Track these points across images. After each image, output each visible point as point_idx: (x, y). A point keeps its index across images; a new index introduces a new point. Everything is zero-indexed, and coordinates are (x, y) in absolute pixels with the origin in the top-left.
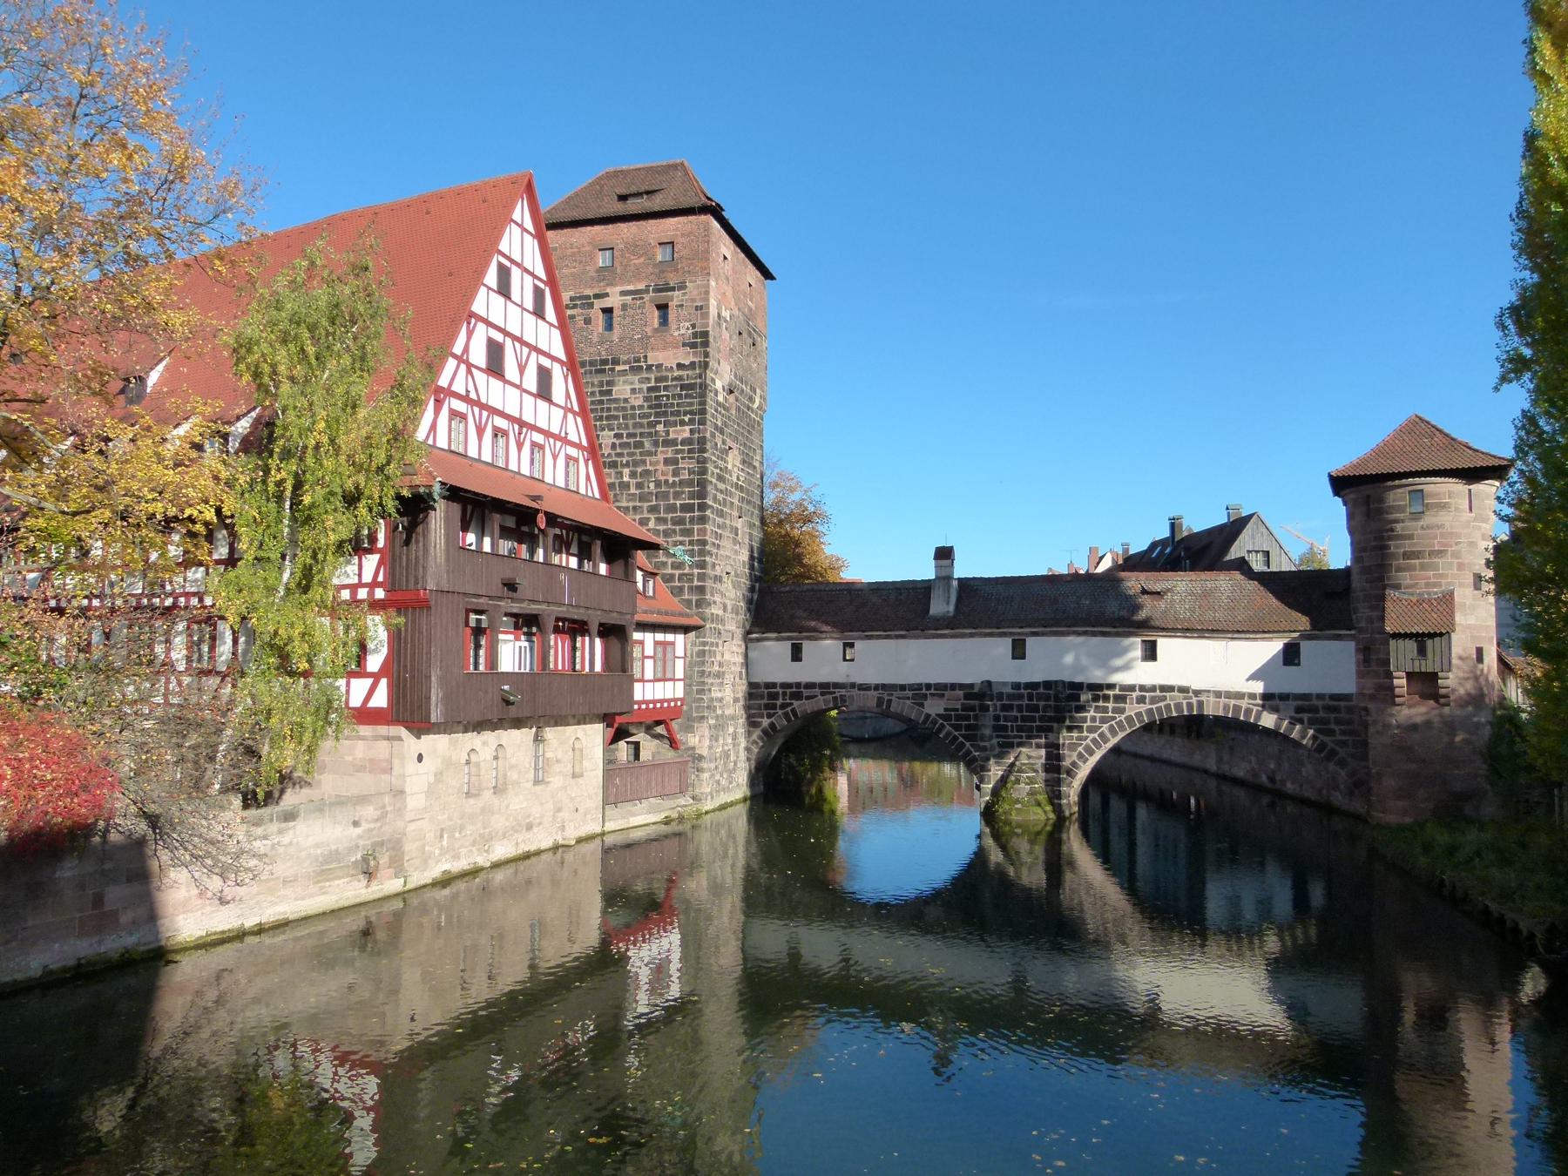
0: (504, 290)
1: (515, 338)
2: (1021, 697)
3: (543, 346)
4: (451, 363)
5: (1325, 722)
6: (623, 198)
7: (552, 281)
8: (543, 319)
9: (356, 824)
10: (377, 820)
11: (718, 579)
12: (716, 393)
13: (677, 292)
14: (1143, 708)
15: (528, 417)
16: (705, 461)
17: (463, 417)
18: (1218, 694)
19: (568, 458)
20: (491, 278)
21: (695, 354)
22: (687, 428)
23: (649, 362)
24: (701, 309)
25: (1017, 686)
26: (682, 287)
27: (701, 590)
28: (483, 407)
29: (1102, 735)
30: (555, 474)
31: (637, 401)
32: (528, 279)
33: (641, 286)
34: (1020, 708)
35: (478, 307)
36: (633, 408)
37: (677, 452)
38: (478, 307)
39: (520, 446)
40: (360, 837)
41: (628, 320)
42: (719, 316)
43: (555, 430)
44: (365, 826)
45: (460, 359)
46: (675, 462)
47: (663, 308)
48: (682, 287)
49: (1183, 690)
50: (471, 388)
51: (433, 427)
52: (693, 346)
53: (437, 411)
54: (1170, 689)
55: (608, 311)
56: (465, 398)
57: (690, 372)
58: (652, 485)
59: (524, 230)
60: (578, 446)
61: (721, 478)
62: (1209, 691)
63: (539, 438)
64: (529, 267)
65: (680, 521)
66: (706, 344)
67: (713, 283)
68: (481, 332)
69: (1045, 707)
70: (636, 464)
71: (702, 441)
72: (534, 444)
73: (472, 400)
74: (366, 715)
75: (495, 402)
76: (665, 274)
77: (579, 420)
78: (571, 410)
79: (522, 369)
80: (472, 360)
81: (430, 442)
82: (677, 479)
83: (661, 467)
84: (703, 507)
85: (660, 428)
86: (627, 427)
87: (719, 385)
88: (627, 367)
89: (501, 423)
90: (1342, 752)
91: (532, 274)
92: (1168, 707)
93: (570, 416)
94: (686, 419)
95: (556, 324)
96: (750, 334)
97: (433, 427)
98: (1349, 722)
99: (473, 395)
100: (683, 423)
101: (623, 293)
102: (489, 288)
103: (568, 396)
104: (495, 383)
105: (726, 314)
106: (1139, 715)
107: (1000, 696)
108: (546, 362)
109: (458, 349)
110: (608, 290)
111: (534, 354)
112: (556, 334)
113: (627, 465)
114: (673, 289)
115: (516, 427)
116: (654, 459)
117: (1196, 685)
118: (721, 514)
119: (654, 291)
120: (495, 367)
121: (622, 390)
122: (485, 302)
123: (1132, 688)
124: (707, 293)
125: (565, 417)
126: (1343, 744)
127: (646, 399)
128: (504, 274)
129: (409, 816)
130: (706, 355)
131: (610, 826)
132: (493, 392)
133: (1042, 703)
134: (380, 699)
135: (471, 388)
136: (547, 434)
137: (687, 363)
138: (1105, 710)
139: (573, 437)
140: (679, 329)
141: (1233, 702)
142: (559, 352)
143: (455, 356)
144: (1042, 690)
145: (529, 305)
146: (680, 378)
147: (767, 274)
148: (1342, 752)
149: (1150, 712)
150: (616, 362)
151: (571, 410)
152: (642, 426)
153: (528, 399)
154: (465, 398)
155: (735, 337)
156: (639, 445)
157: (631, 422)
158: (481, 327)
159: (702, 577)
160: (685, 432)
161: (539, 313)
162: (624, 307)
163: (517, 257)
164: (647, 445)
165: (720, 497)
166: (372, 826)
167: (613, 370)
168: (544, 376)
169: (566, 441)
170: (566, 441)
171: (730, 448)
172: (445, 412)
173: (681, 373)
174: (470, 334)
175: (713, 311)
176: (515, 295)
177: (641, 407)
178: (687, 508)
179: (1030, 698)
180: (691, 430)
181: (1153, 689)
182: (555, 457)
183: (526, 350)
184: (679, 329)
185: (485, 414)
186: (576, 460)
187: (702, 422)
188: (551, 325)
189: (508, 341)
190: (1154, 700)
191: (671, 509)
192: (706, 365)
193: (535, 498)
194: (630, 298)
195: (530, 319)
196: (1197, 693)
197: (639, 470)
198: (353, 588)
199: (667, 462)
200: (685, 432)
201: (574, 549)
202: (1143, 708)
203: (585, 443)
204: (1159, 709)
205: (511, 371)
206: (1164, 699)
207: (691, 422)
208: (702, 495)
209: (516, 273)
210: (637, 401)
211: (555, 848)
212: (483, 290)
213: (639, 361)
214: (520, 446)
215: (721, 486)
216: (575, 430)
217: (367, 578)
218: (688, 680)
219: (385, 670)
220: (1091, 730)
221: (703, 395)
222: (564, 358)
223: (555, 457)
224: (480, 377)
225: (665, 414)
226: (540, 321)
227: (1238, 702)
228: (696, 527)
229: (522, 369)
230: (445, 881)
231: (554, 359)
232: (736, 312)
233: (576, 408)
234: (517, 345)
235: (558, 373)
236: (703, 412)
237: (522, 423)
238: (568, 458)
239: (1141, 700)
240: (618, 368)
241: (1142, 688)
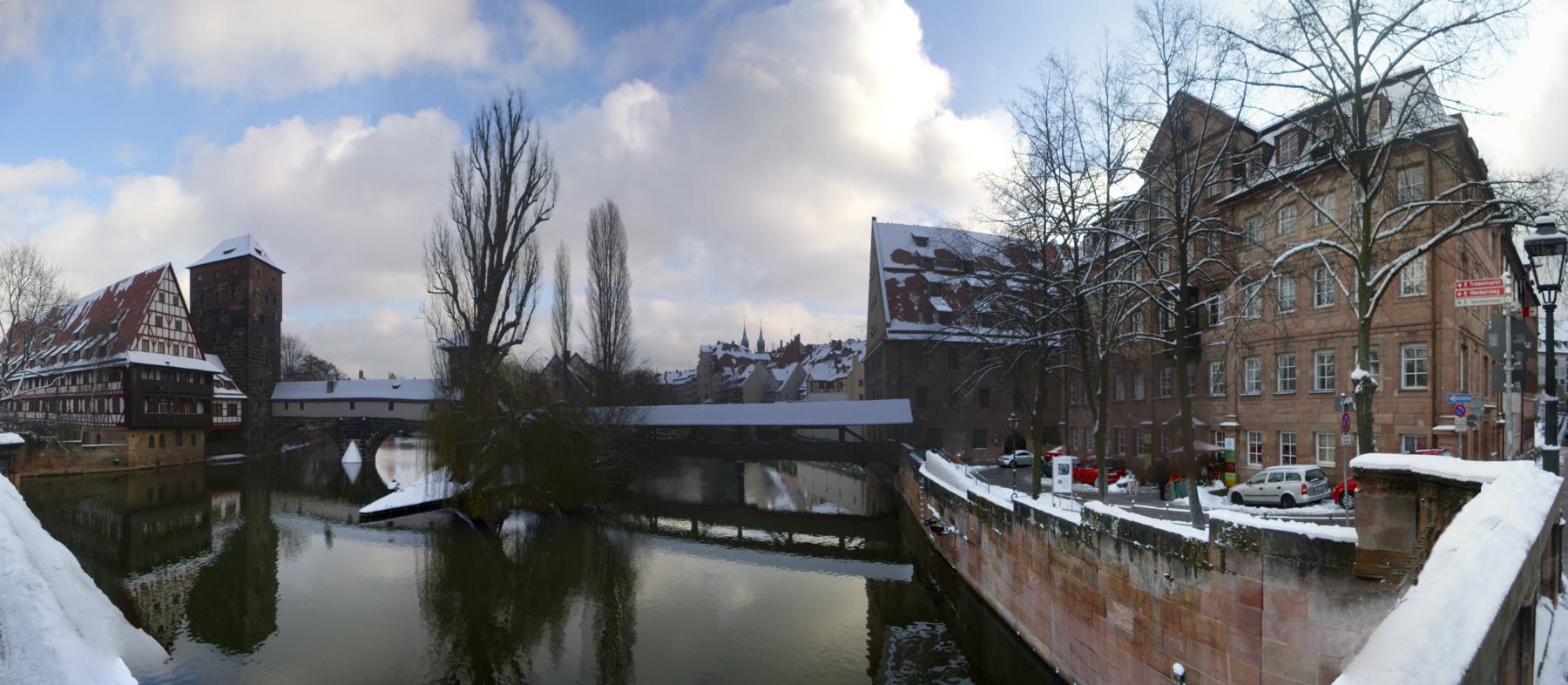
0: (162, 300)
1: (166, 314)
3: (178, 314)
4: (143, 326)
6: (226, 253)
12: (254, 318)
15: (172, 337)
17: (148, 341)
19: (189, 348)
20: (157, 298)
24: (247, 290)
28: (154, 337)
31: (227, 323)
33: (226, 284)
35: (152, 308)
39: (169, 346)
42: (255, 291)
43: (183, 339)
45: (146, 325)
47: (233, 291)
53: (138, 340)
55: (217, 293)
59: (169, 280)
60: (193, 343)
61: (255, 347)
64: (171, 291)
67: (251, 281)
68: (153, 316)
72: (174, 345)
74: (119, 424)
75: (159, 334)
79: (169, 323)
85: (234, 332)
87: (255, 315)
99: (151, 334)
103: (188, 328)
104: (159, 330)
105: (258, 290)
108: (179, 319)
109: (145, 321)
112: (183, 310)
121: (222, 320)
122: (156, 306)
125: (187, 336)
131: (207, 460)
132: (159, 332)
134: (123, 421)
136: (180, 341)
139: (190, 340)
142: (184, 315)
145: (172, 303)
153: (172, 333)
154: (148, 335)
155: (263, 299)
158: (154, 313)
160: (241, 333)
161: (176, 304)
163: (166, 289)
169: (187, 342)
170: (187, 342)
172: (141, 341)
174: (149, 316)
175: (251, 288)
176: (166, 301)
178: (243, 359)
182: (183, 348)
186: (192, 348)
192: (248, 309)
193: (167, 363)
195: (172, 308)
198: (117, 391)
199: (237, 344)
200: (241, 333)
201: (192, 375)
203: (195, 342)
205: (165, 324)
209: (166, 294)
210: (227, 323)
211: (184, 465)
212: (153, 303)
214: (169, 346)
216: (191, 338)
217: (119, 388)
218: (242, 416)
219: (124, 413)
222: (186, 316)
223: (183, 348)
224: (153, 329)
229: (169, 323)
230: (142, 469)
231: (182, 318)
237: (169, 339)
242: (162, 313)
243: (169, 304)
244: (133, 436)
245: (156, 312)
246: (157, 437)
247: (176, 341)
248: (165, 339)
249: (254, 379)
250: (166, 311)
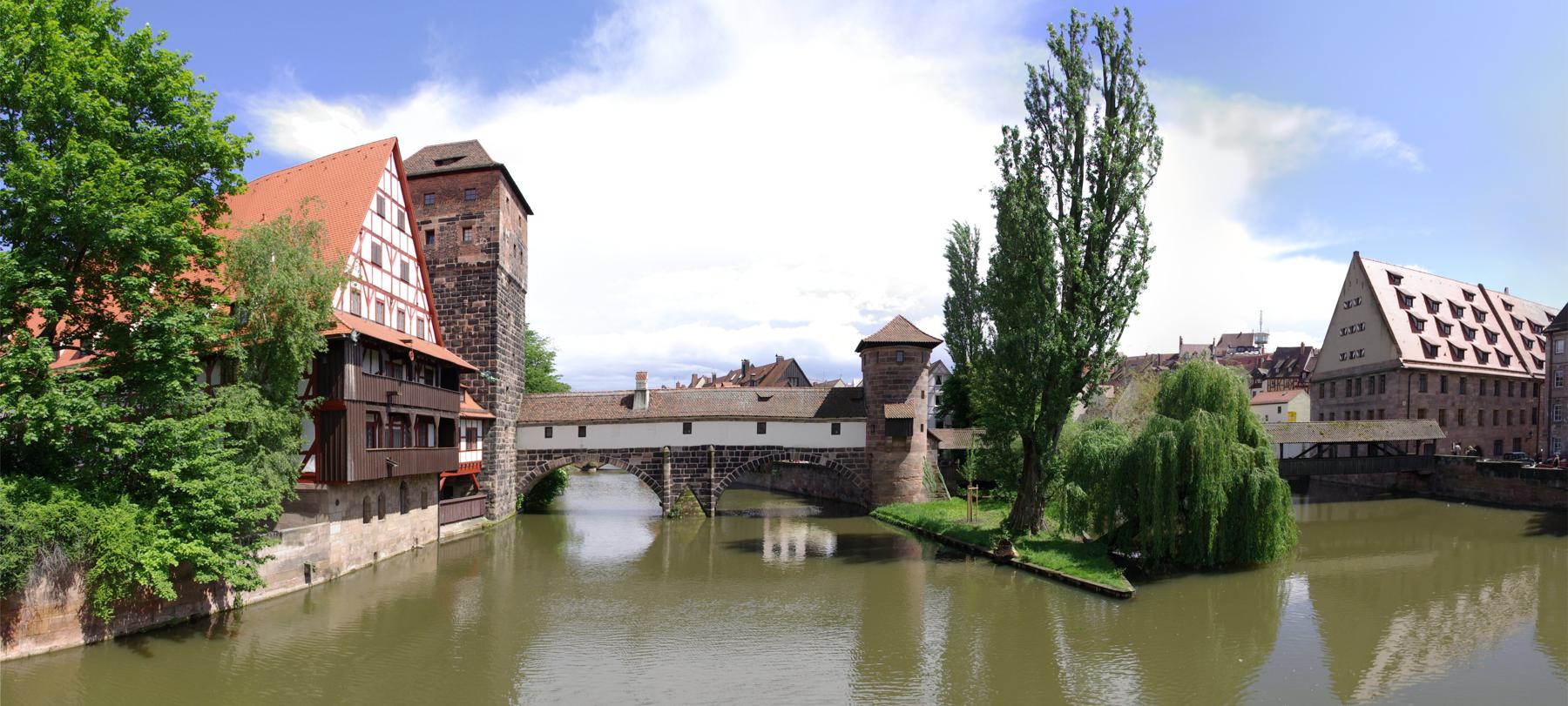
2: (688, 454)
3: (404, 248)
5: (851, 461)
6: (439, 163)
7: (407, 209)
8: (404, 232)
9: (301, 544)
10: (313, 541)
11: (502, 391)
13: (477, 220)
14: (757, 458)
15: (396, 293)
16: (493, 322)
18: (798, 450)
20: (374, 206)
21: (490, 257)
22: (484, 302)
23: (459, 262)
24: (495, 229)
25: (685, 448)
26: (481, 216)
27: (493, 398)
29: (734, 473)
30: (411, 329)
32: (395, 207)
33: (454, 215)
34: (687, 461)
35: (366, 224)
36: (448, 290)
37: (478, 316)
38: (366, 224)
40: (304, 551)
41: (445, 237)
42: (504, 233)
44: (306, 545)
46: (476, 322)
48: (481, 216)
49: (780, 448)
50: (363, 274)
51: (341, 299)
52: (488, 252)
53: (344, 288)
54: (773, 447)
56: (359, 280)
57: (486, 268)
58: (460, 337)
60: (423, 311)
62: (793, 448)
63: (402, 306)
64: (395, 199)
65: (479, 357)
66: (497, 251)
67: (501, 214)
68: (368, 238)
69: (702, 459)
70: (449, 324)
71: (494, 311)
73: (363, 282)
75: (377, 283)
76: (470, 208)
77: (424, 295)
78: (420, 289)
80: (363, 257)
81: (340, 308)
82: (477, 333)
83: (467, 326)
84: (494, 349)
86: (443, 302)
88: (444, 265)
89: (381, 296)
90: (858, 476)
91: (396, 203)
92: (771, 457)
93: (419, 292)
94: (484, 296)
95: (411, 235)
96: (519, 246)
97: (341, 299)
98: (862, 461)
99: (364, 279)
100: (481, 299)
101: (440, 220)
102: (373, 211)
103: (418, 280)
105: (508, 233)
106: (755, 462)
107: (676, 454)
108: (405, 259)
109: (355, 250)
110: (431, 218)
111: (398, 254)
112: (411, 241)
113: (444, 324)
114: (475, 217)
115: (389, 299)
116: (462, 320)
117: (785, 446)
118: (504, 353)
119: (462, 219)
120: (376, 264)
122: (371, 221)
123: (752, 448)
124: (498, 219)
126: (858, 472)
127: (457, 285)
128: (381, 202)
129: (332, 538)
130: (497, 257)
132: (375, 277)
133: (700, 457)
135: (363, 274)
137: (484, 262)
138: (737, 460)
139: (421, 305)
140: (478, 241)
141: (805, 453)
143: (354, 254)
144: (700, 450)
146: (479, 271)
147: (531, 213)
148: (858, 476)
149: (760, 460)
150: (436, 262)
151: (420, 289)
152: (454, 301)
156: (453, 313)
157: (446, 299)
159: (494, 390)
162: (442, 229)
164: (457, 311)
165: (504, 342)
166: (311, 544)
167: (434, 267)
168: (404, 266)
170: (416, 307)
171: (509, 315)
173: (480, 268)
175: (501, 231)
176: (388, 216)
177: (453, 289)
178: (482, 349)
179: (693, 454)
180: (487, 304)
181: (763, 447)
183: (394, 251)
184: (478, 241)
185: (371, 290)
187: (494, 299)
188: (408, 235)
189: (384, 245)
190: (763, 454)
191: (474, 350)
194: (445, 223)
196: (787, 449)
197: (452, 327)
202: (757, 458)
203: (428, 310)
204: (766, 458)
205: (386, 264)
206: (770, 453)
207: (486, 298)
208: (494, 342)
209: (388, 202)
212: (369, 212)
213: (452, 261)
214: (391, 310)
215: (504, 336)
216: (422, 301)
220: (728, 471)
221: (495, 283)
223: (411, 317)
224: (368, 267)
225: (469, 294)
226: (402, 233)
227: (808, 453)
228: (490, 361)
229: (391, 262)
231: (410, 257)
232: (513, 233)
233: (423, 288)
234: (389, 248)
235: (413, 265)
236: (495, 293)
237: (392, 297)
238: (419, 320)
239: (757, 454)
240: (438, 266)
241: (758, 448)
242: (383, 240)
243: (391, 223)
244: (337, 503)
245: (371, 232)
246: (373, 499)
247: (402, 301)
248: (385, 293)
249: (502, 387)
250: (387, 237)
